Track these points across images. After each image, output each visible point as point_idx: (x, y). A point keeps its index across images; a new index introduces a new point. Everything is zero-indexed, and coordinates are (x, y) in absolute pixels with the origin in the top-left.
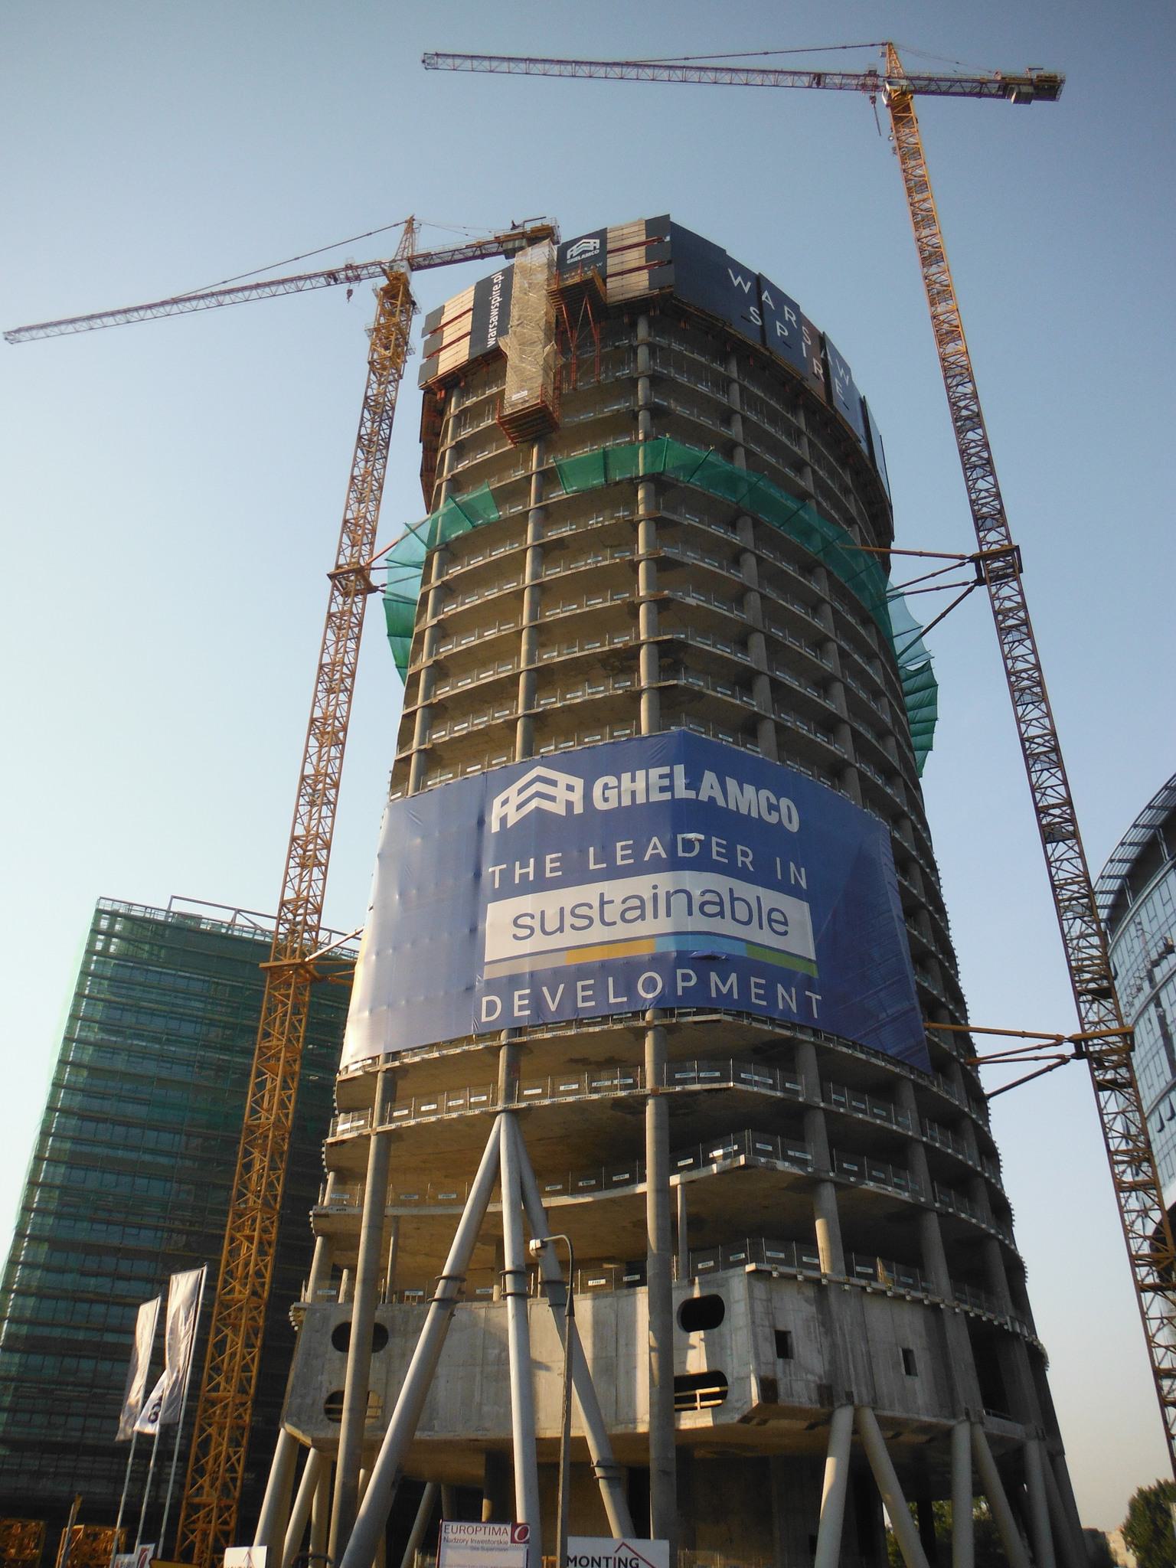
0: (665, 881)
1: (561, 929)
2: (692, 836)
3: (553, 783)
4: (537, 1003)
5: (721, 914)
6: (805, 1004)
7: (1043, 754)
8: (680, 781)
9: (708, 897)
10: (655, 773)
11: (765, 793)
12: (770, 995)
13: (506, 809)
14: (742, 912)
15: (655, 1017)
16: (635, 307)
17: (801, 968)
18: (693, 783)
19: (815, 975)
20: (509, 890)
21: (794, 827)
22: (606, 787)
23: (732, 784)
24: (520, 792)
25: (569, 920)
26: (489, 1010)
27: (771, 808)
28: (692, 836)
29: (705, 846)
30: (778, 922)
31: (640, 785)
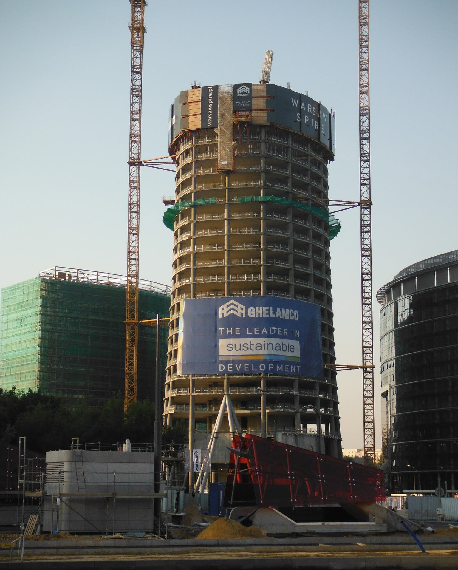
0: (267, 340)
1: (240, 349)
4: (234, 368)
5: (280, 350)
6: (297, 369)
7: (366, 252)
8: (271, 312)
9: (278, 345)
10: (265, 308)
11: (291, 310)
12: (289, 369)
13: (223, 311)
14: (284, 349)
15: (264, 375)
16: (261, 126)
18: (274, 313)
20: (226, 336)
21: (297, 319)
22: (252, 310)
23: (283, 310)
24: (228, 306)
25: (242, 347)
26: (221, 368)
27: (293, 315)
31: (261, 312)
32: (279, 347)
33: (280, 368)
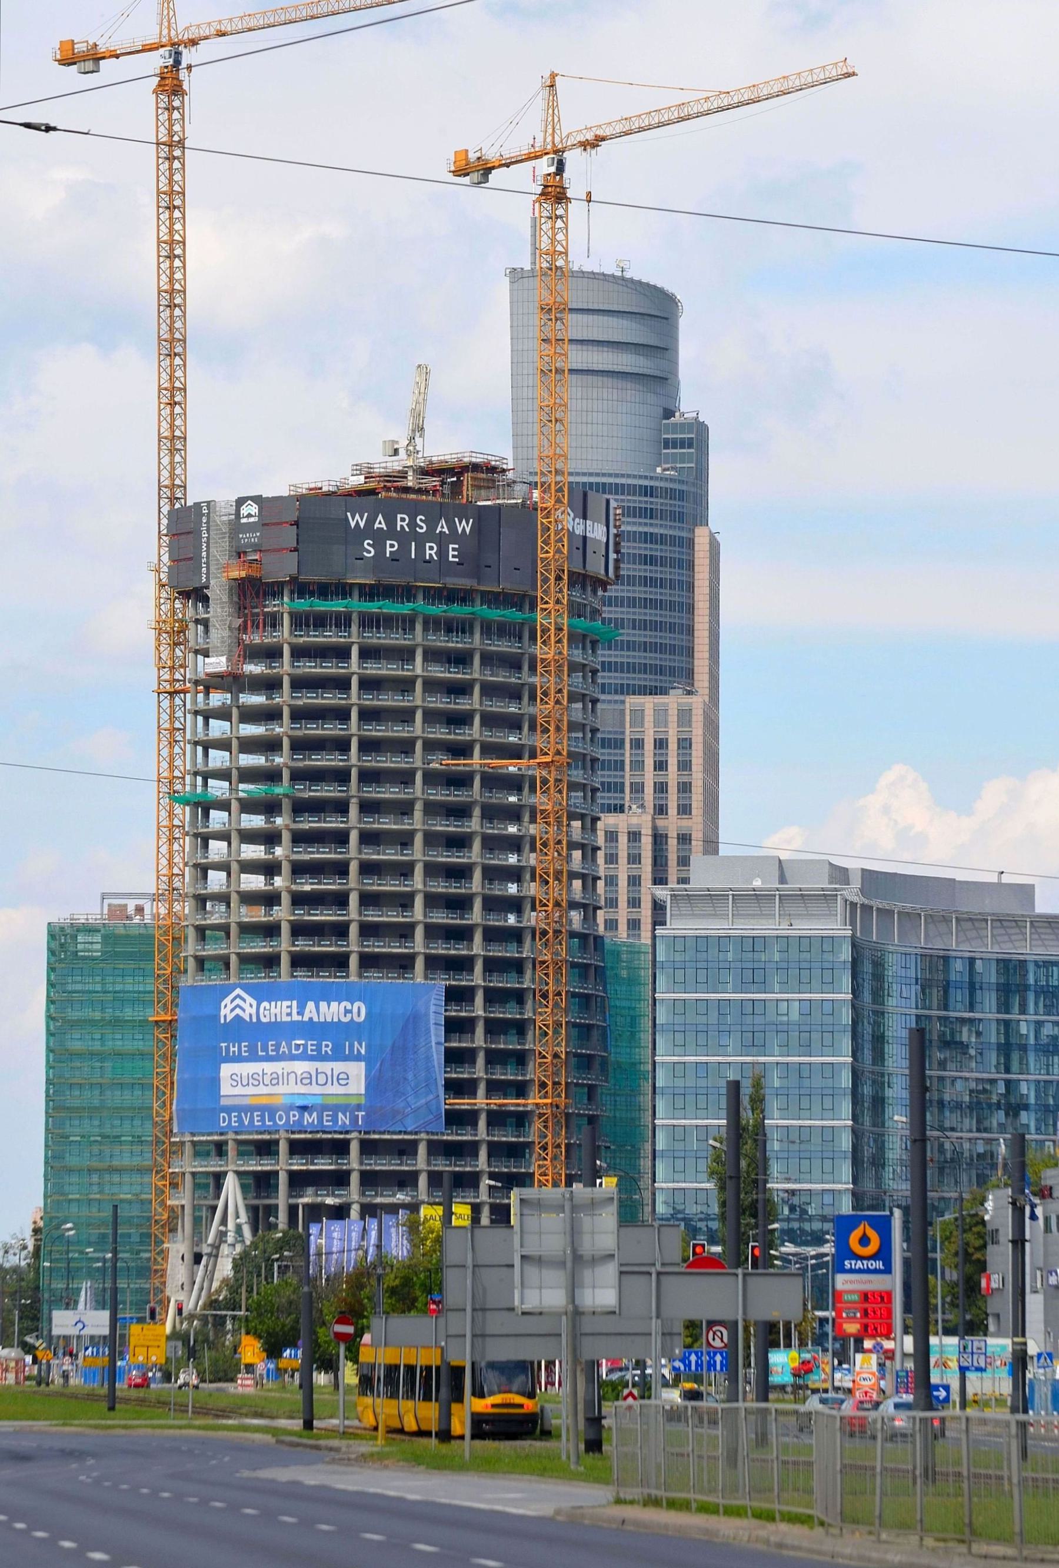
3: (244, 1001)
4: (240, 1120)
8: (295, 1011)
9: (305, 1075)
17: (354, 1101)
18: (300, 1013)
19: (363, 1102)
22: (265, 1009)
23: (323, 1005)
25: (251, 1081)
27: (347, 1011)
29: (305, 1046)
30: (343, 1079)
32: (308, 1079)
33: (310, 1119)
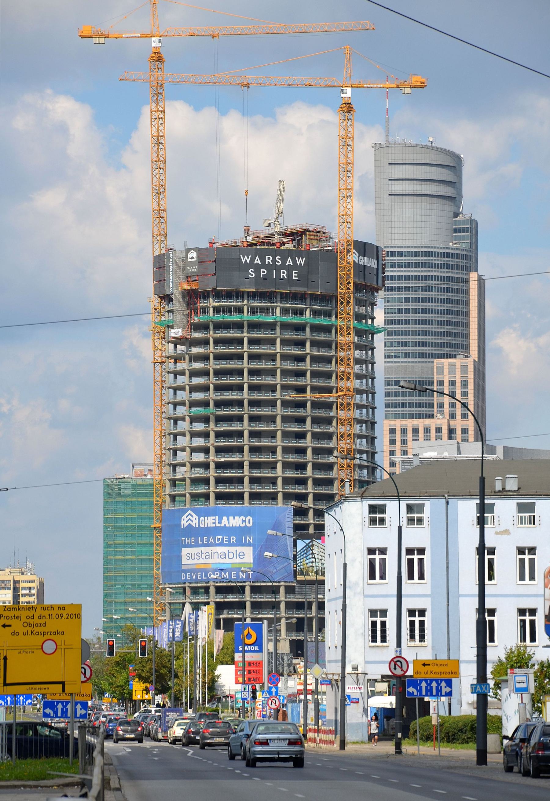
2: (219, 537)
23: (231, 518)
28: (219, 537)
29: (222, 539)
